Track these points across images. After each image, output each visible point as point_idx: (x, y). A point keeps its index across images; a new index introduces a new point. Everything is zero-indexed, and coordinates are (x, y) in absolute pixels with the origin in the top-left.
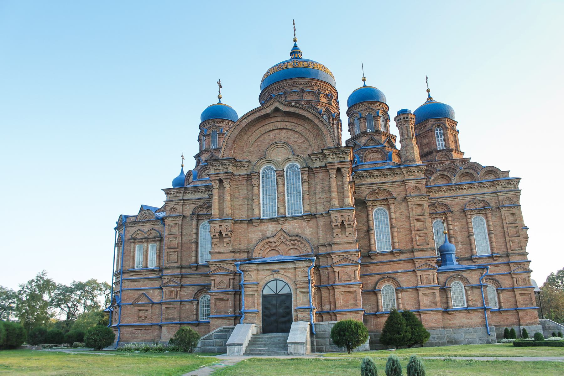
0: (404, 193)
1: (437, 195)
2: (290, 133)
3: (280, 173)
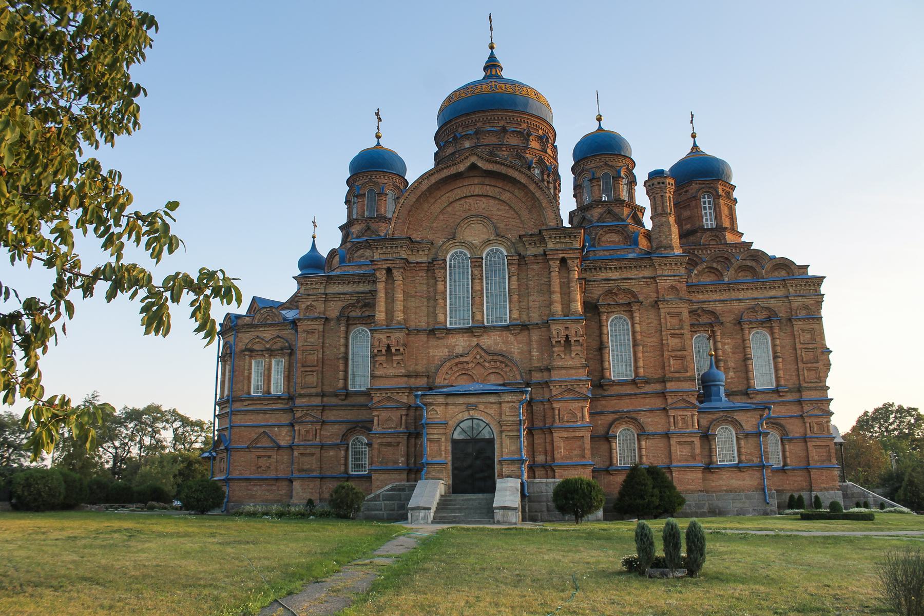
0: (654, 295)
1: (700, 297)
2: (491, 202)
3: (477, 262)
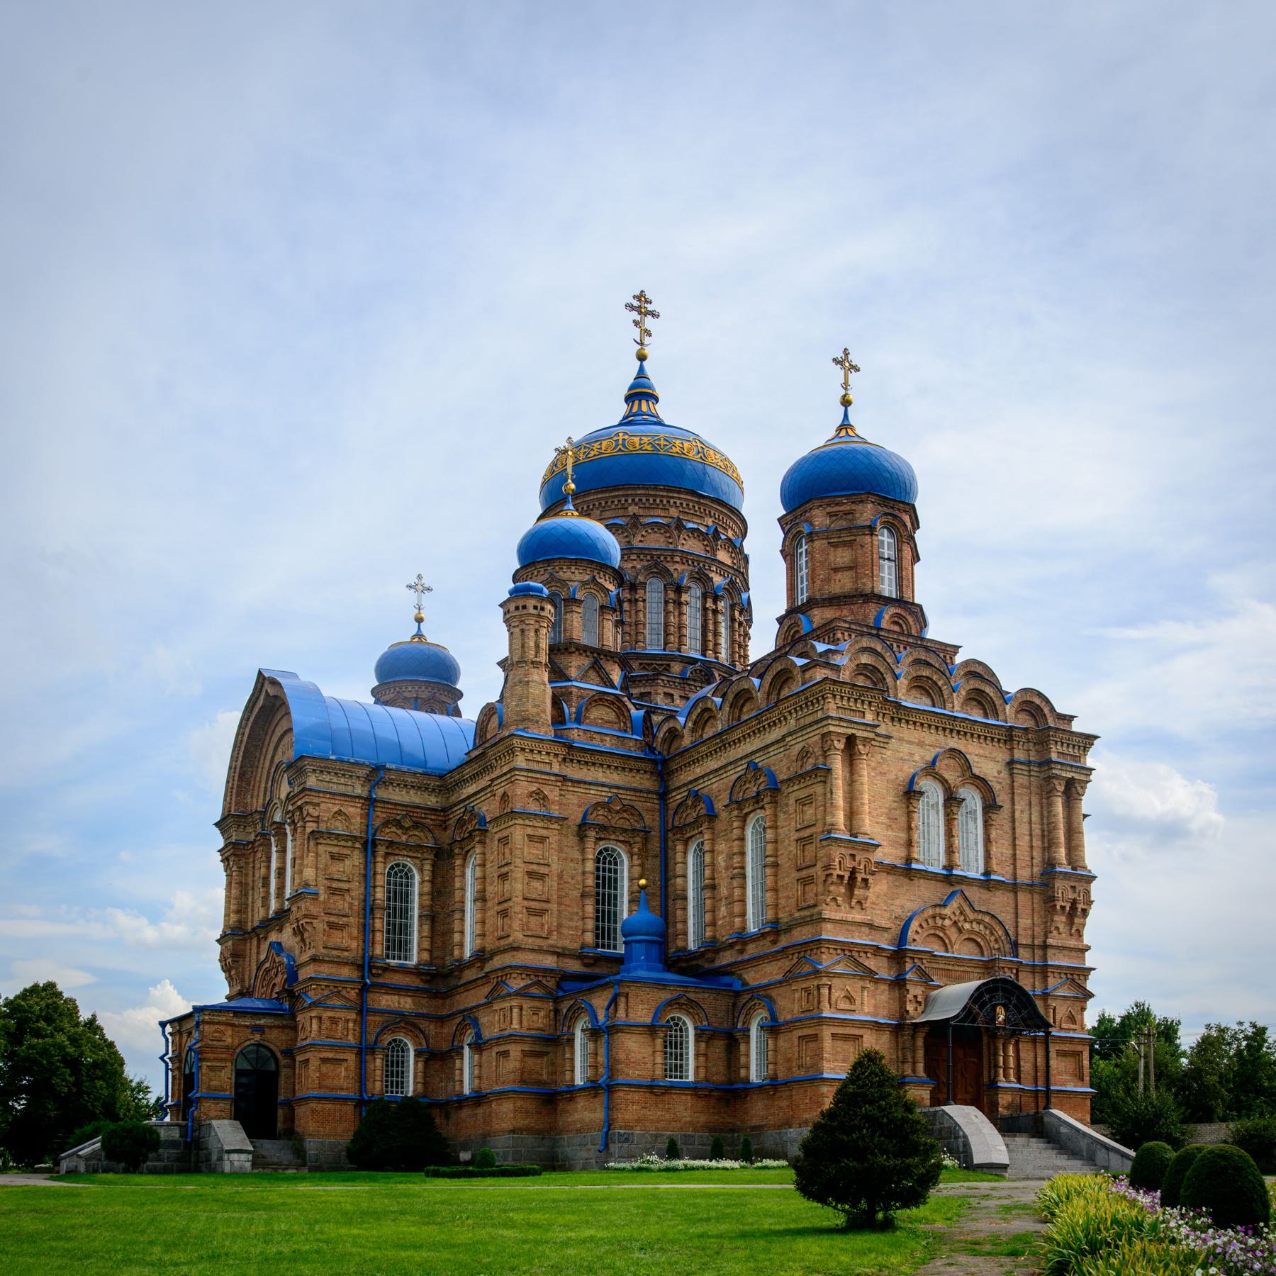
1: (698, 771)
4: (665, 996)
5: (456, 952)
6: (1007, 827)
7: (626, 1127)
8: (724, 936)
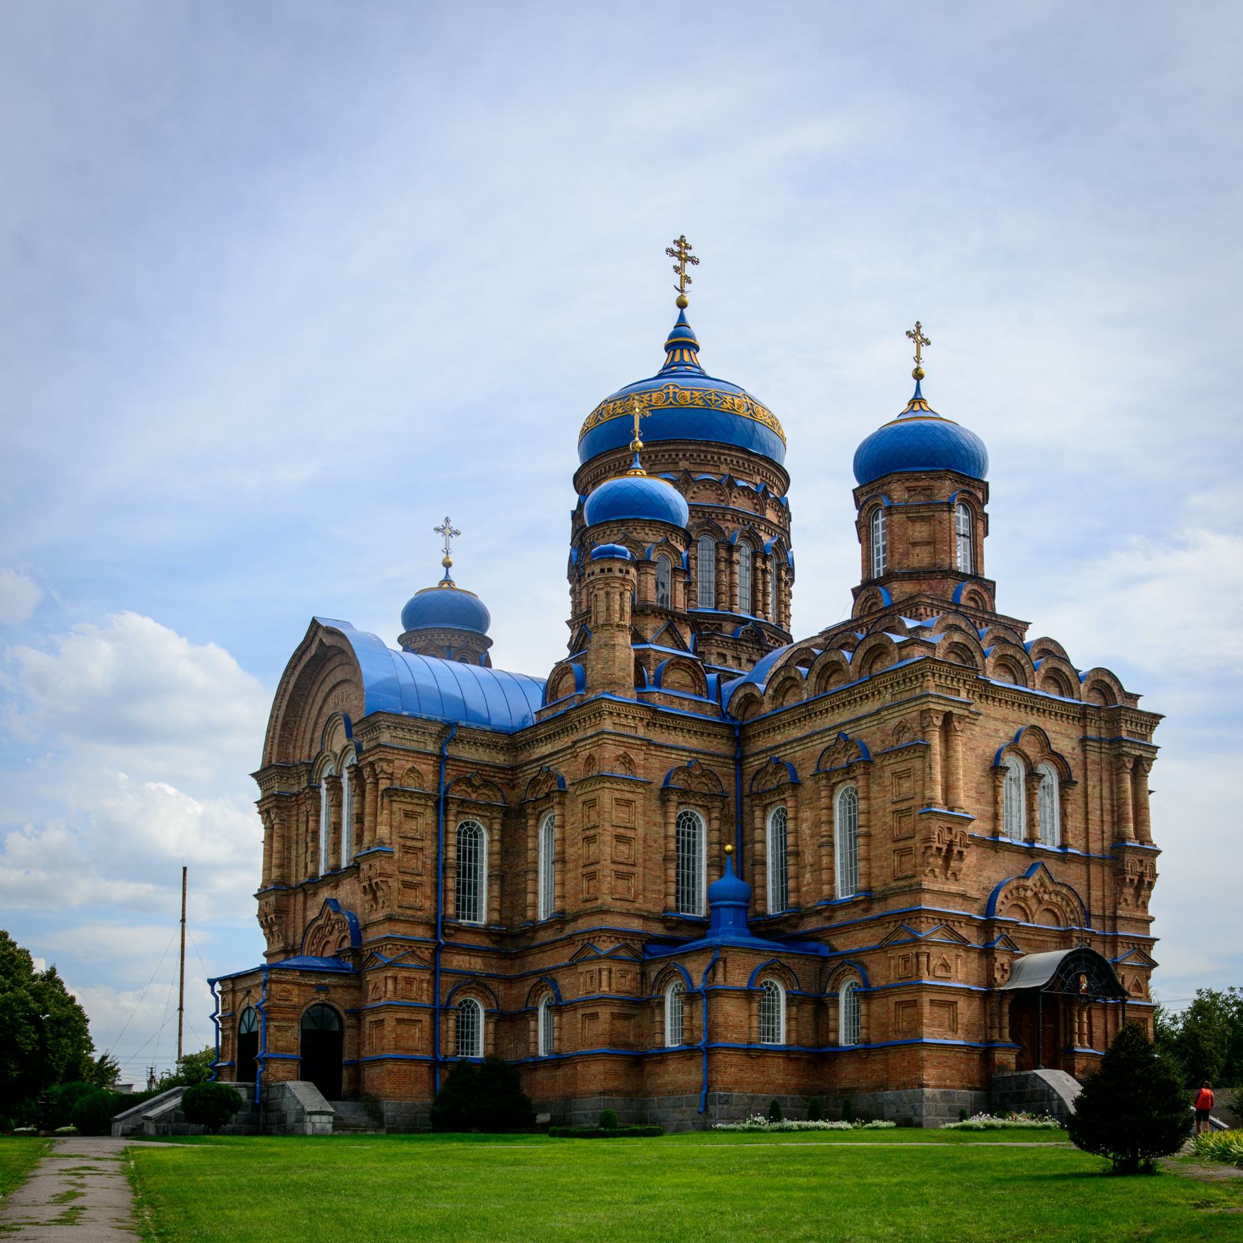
1: (779, 738)
4: (759, 961)
5: (530, 913)
6: (1080, 801)
7: (725, 1089)
8: (810, 902)
